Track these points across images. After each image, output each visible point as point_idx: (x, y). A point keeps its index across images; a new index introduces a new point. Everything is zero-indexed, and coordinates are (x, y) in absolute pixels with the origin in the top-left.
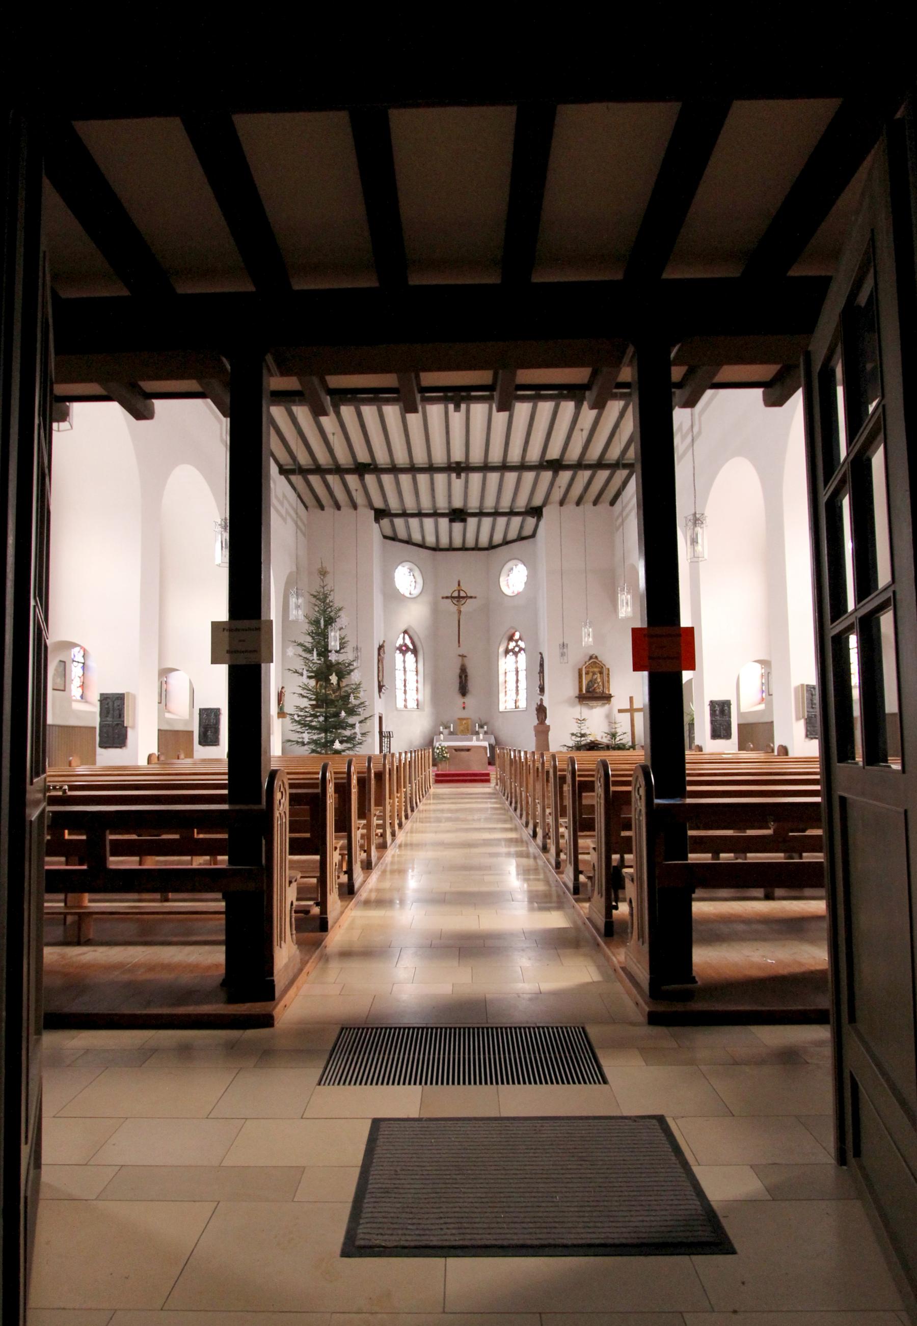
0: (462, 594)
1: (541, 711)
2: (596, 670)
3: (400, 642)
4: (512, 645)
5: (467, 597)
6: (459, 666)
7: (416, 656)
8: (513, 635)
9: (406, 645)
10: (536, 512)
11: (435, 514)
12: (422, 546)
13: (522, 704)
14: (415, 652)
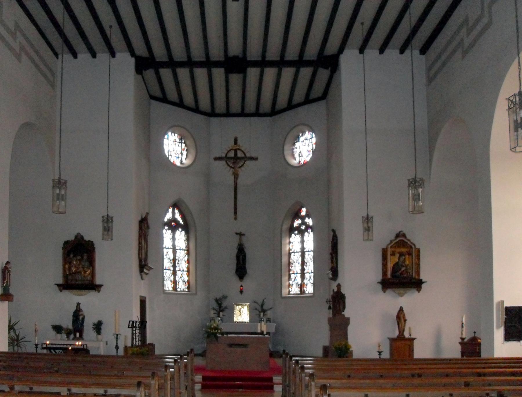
1: (338, 301)
2: (404, 250)
3: (169, 216)
4: (297, 223)
5: (245, 158)
6: (236, 245)
7: (187, 233)
8: (300, 211)
10: (330, 63)
11: (208, 64)
12: (196, 110)
13: (309, 289)
14: (186, 228)
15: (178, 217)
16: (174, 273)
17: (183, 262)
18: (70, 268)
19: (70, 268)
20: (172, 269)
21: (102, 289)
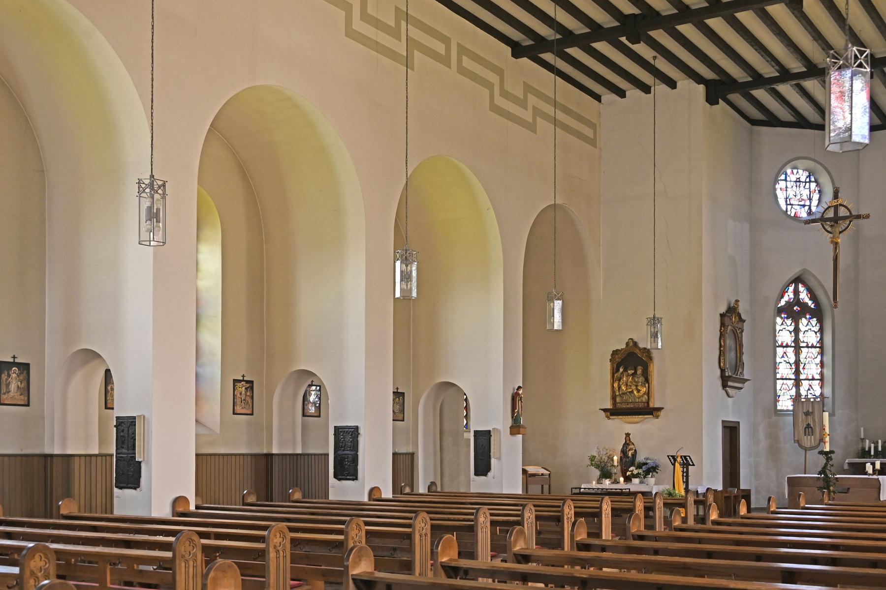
0: (842, 212)
3: (789, 295)
5: (851, 217)
7: (820, 321)
9: (797, 301)
14: (817, 313)
15: (804, 296)
16: (797, 383)
17: (813, 366)
18: (619, 388)
19: (619, 388)
20: (793, 377)
21: (662, 413)
